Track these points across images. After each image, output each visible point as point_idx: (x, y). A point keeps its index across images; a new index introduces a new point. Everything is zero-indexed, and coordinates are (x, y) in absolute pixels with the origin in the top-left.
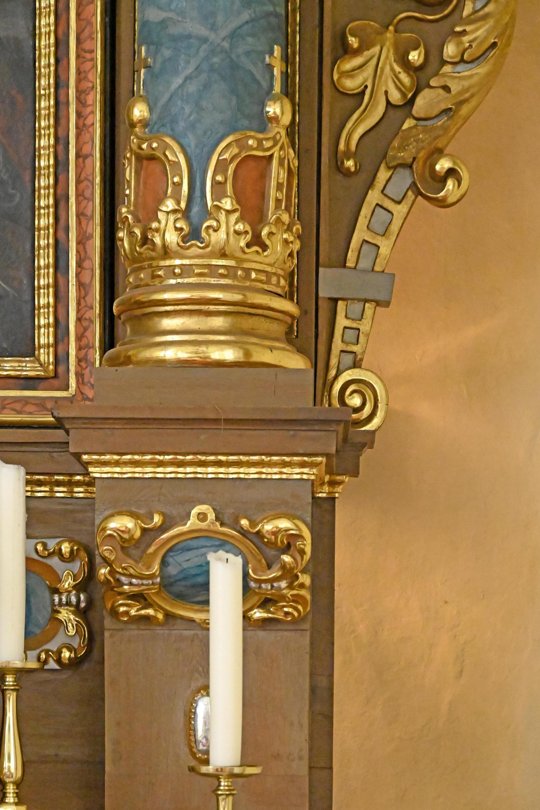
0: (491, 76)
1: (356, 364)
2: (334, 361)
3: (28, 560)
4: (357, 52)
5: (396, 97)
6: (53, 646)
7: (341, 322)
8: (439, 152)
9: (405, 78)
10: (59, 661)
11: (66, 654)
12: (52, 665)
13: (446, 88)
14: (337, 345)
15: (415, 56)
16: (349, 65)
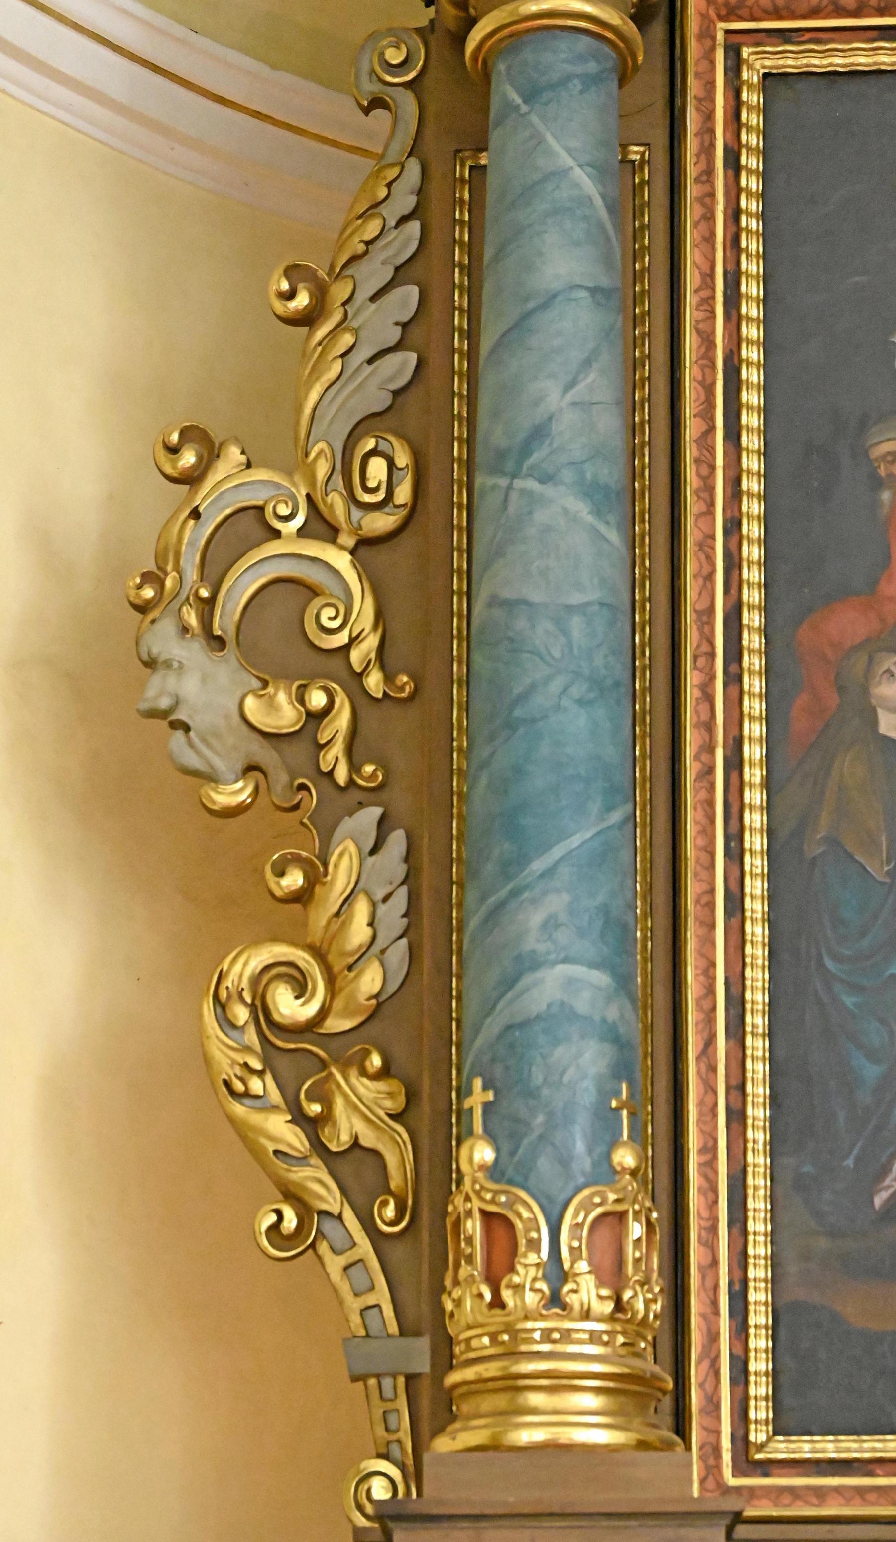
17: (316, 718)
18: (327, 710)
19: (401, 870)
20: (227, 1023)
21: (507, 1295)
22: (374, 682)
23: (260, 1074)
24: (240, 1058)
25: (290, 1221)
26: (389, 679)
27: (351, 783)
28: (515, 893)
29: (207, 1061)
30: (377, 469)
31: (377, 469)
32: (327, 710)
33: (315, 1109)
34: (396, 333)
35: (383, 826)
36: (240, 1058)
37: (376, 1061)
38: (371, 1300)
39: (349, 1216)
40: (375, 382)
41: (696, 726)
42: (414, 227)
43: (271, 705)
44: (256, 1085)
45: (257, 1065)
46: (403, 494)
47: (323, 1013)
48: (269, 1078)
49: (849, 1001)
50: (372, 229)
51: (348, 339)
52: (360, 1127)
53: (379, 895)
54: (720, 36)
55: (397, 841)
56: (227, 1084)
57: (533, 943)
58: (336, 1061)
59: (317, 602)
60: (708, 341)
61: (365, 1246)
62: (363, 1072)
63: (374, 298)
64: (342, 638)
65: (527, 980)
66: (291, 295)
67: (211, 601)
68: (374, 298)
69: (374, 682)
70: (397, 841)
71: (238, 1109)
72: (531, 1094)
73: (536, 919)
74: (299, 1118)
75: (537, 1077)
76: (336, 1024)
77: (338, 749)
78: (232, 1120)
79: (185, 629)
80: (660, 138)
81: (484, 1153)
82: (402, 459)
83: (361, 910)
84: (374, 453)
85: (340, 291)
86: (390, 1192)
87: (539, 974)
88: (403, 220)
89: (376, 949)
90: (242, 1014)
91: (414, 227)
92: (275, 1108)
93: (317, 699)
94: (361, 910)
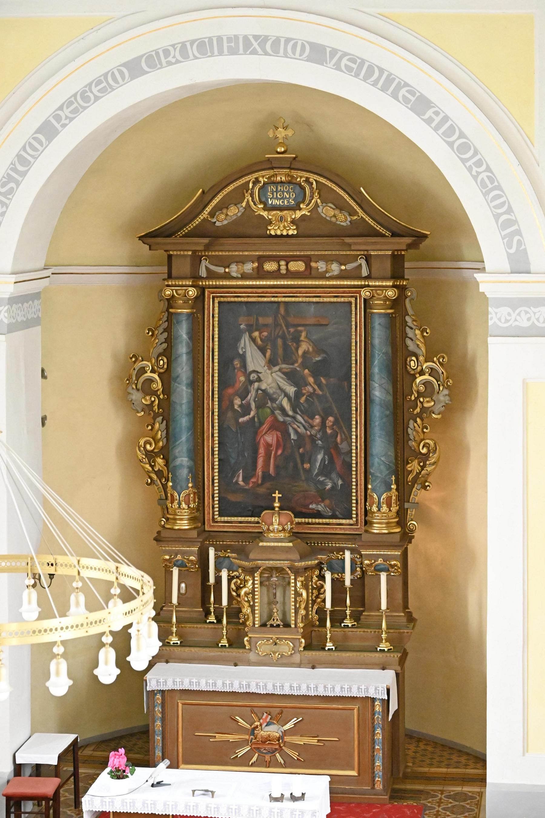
0: (435, 468)
1: (412, 520)
2: (408, 520)
3: (351, 558)
4: (410, 463)
5: (418, 471)
6: (356, 575)
7: (409, 512)
8: (426, 481)
9: (420, 468)
10: (357, 577)
11: (358, 576)
12: (356, 578)
13: (427, 470)
14: (408, 517)
15: (421, 464)
16: (409, 466)
17: (153, 402)
18: (155, 400)
19: (165, 427)
20: (140, 450)
21: (173, 506)
22: (161, 397)
23: (145, 459)
24: (141, 456)
25: (149, 480)
26: (164, 395)
27: (158, 412)
28: (175, 446)
29: (137, 457)
30: (161, 362)
31: (161, 362)
32: (155, 400)
33: (153, 464)
34: (164, 340)
35: (163, 420)
36: (141, 456)
37: (162, 457)
38: (161, 493)
39: (158, 480)
40: (161, 348)
41: (207, 409)
42: (167, 323)
43: (146, 400)
44: (144, 460)
45: (144, 457)
46: (165, 366)
47: (154, 449)
48: (146, 459)
49: (230, 450)
50: (161, 322)
51: (157, 341)
52: (159, 467)
53: (162, 431)
54: (211, 297)
55: (165, 422)
56: (140, 460)
57: (177, 454)
58: (156, 456)
59: (153, 383)
60: (208, 347)
61: (160, 485)
62: (160, 458)
63: (161, 334)
64: (157, 389)
65: (176, 460)
66: (148, 333)
67: (137, 383)
68: (161, 334)
69: (161, 397)
70: (165, 422)
71: (142, 464)
72: (177, 477)
73: (177, 451)
74: (151, 466)
75: (177, 474)
76: (156, 451)
77: (156, 407)
78: (141, 466)
79: (133, 388)
80: (202, 314)
81: (171, 484)
82: (165, 360)
83: (160, 433)
84: (161, 360)
85: (156, 332)
86: (164, 477)
87: (178, 459)
88: (165, 322)
89: (162, 439)
90: (142, 449)
91: (167, 323)
92: (147, 463)
93: (153, 399)
94: (160, 433)
